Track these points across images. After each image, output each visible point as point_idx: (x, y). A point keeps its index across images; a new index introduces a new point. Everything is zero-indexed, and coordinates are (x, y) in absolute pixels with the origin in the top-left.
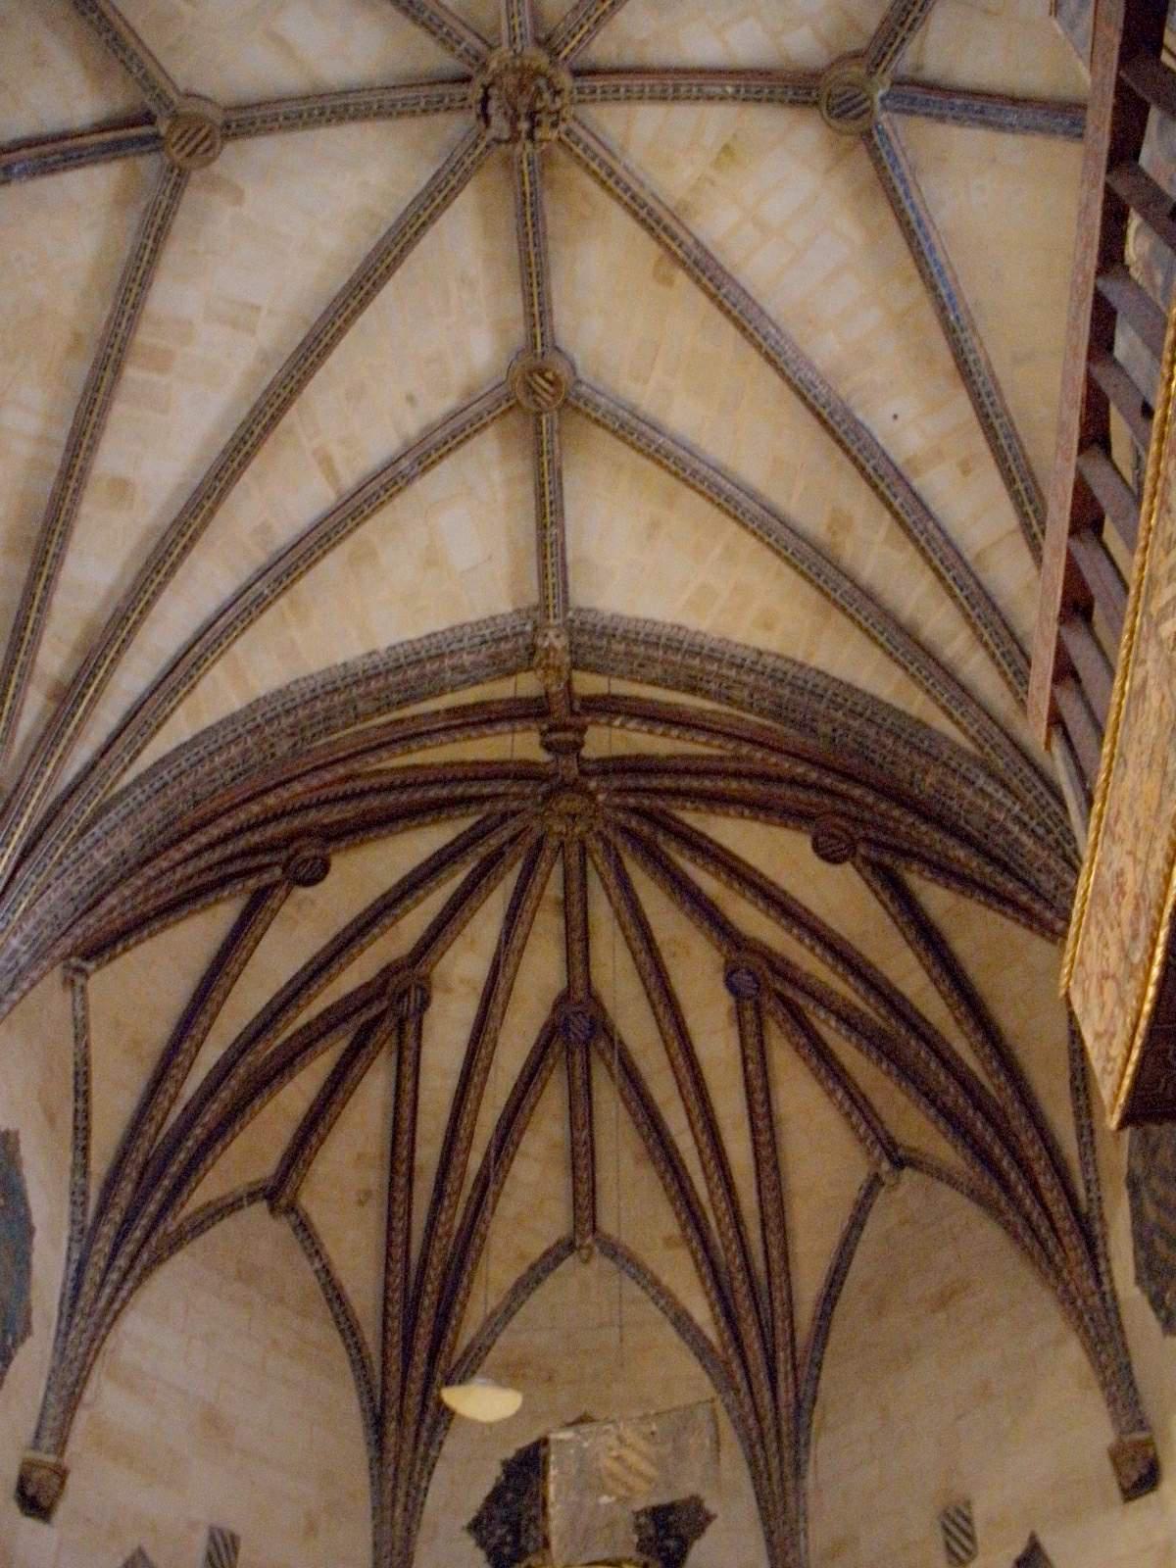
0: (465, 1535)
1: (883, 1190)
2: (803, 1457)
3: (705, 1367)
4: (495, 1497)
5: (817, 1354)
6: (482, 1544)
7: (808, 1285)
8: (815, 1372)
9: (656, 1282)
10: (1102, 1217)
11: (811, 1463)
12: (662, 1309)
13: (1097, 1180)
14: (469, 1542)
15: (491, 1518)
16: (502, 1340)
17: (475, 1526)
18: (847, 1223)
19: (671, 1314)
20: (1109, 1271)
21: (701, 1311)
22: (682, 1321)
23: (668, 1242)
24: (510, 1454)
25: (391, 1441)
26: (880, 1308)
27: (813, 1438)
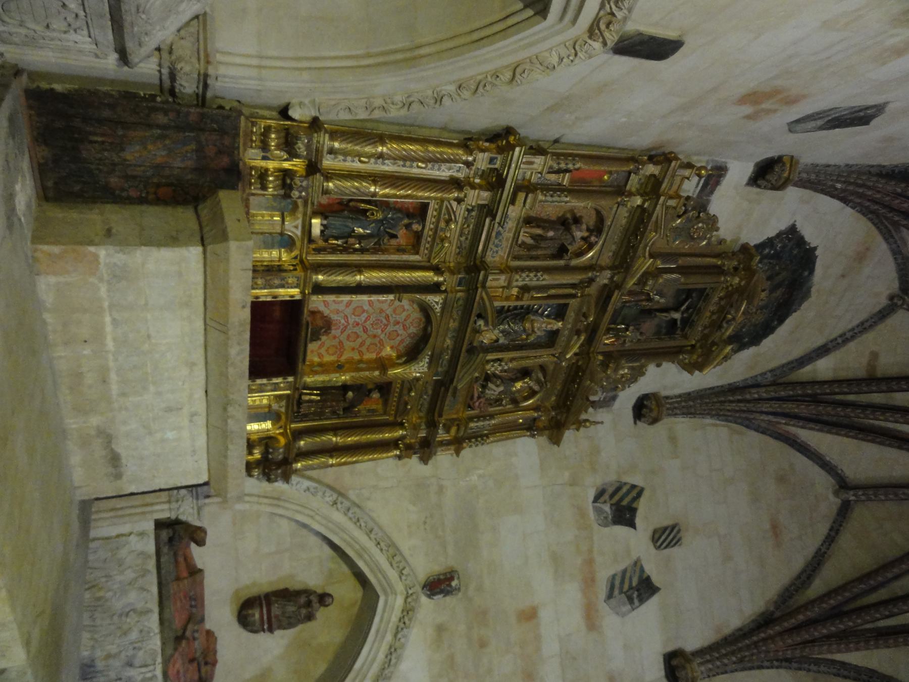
0: (791, 222)
1: (833, 481)
2: (720, 418)
3: (792, 362)
4: (800, 241)
5: (769, 432)
6: (778, 235)
7: (808, 436)
8: (761, 430)
9: (853, 338)
10: (800, 669)
11: (718, 422)
12: (836, 339)
13: (819, 672)
14: (783, 226)
15: (790, 240)
16: (884, 246)
17: (793, 229)
18: (828, 459)
19: (830, 346)
20: (772, 667)
21: (824, 368)
22: (823, 351)
23: (875, 356)
24: (817, 253)
25: (891, 186)
26: (781, 479)
27: (729, 424)
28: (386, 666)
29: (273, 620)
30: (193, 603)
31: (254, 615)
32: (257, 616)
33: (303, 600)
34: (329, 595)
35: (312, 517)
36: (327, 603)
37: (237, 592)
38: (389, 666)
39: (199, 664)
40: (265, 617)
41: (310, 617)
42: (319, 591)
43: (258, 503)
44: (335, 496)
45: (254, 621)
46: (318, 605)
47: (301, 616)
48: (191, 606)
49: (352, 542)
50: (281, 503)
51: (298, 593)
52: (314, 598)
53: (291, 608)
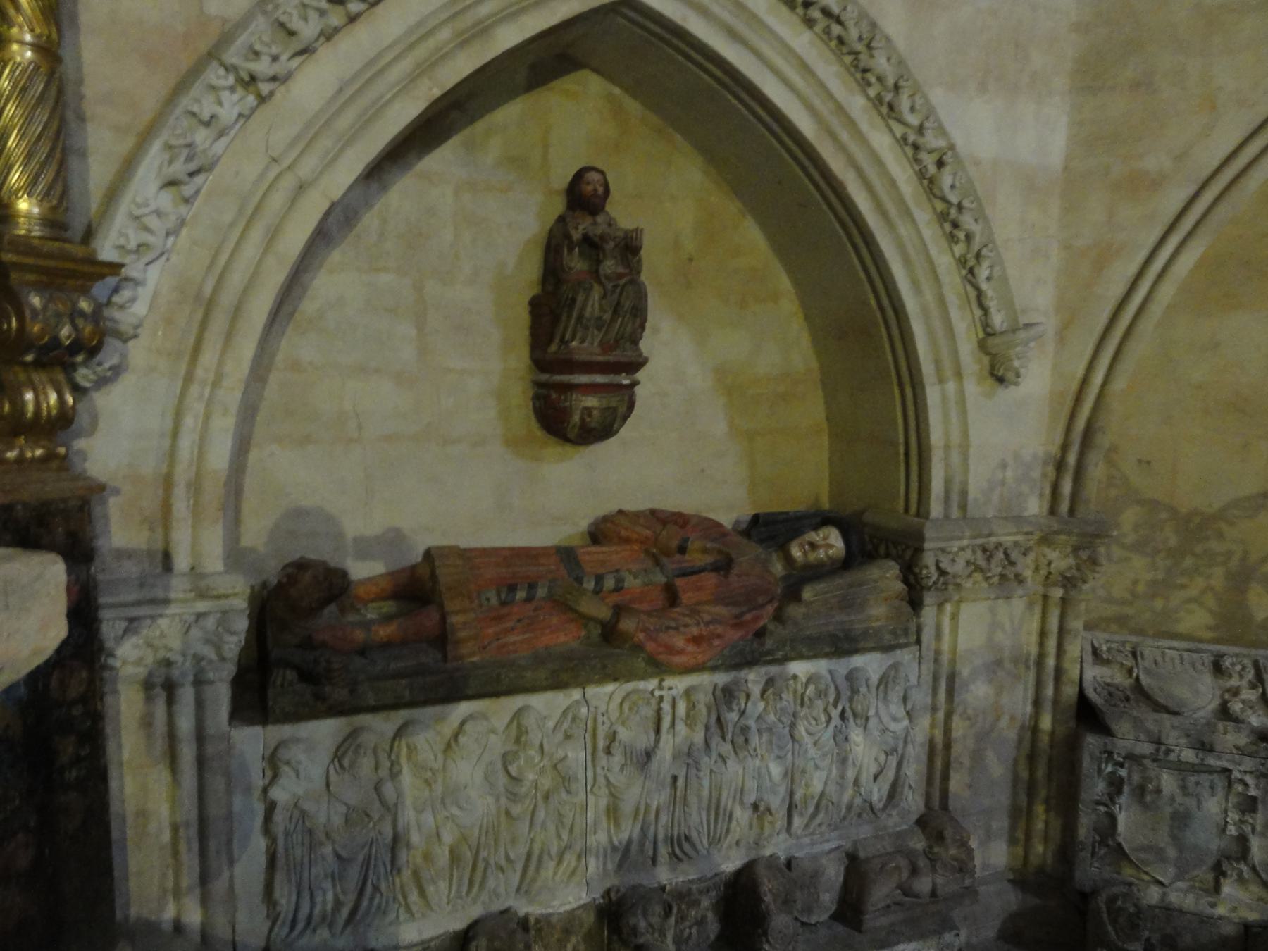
28: (836, 30)
29: (611, 358)
30: (521, 595)
31: (588, 411)
32: (591, 402)
33: (576, 263)
34: (579, 176)
35: (302, 188)
36: (601, 190)
37: (514, 443)
38: (839, 21)
39: (684, 574)
40: (599, 379)
41: (630, 247)
42: (558, 206)
43: (216, 384)
44: (215, 75)
45: (604, 410)
46: (600, 219)
47: (620, 276)
48: (529, 599)
49: (421, 52)
50: (228, 298)
51: (552, 271)
52: (581, 226)
53: (594, 302)
